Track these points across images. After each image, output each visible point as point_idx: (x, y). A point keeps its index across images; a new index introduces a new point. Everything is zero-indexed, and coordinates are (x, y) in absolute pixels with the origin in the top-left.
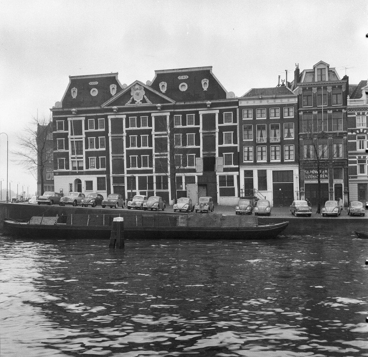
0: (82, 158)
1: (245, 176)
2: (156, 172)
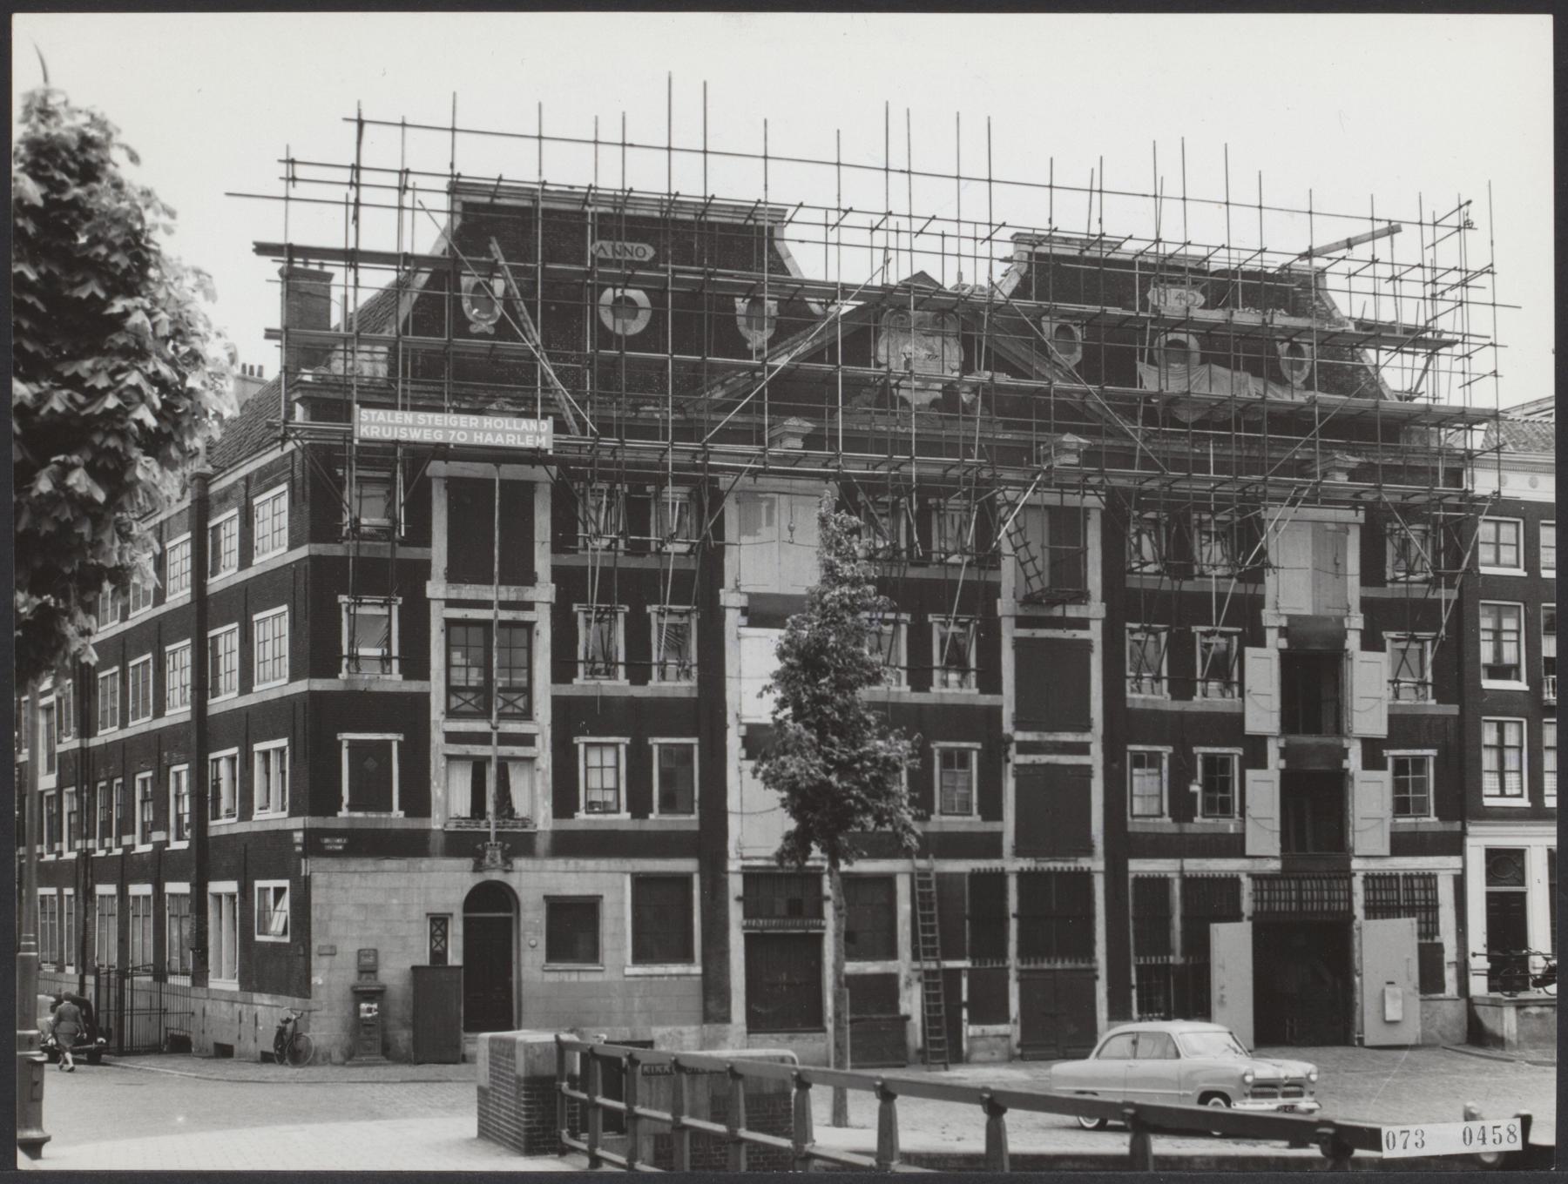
0: (528, 740)
1: (1489, 883)
2: (1019, 852)
